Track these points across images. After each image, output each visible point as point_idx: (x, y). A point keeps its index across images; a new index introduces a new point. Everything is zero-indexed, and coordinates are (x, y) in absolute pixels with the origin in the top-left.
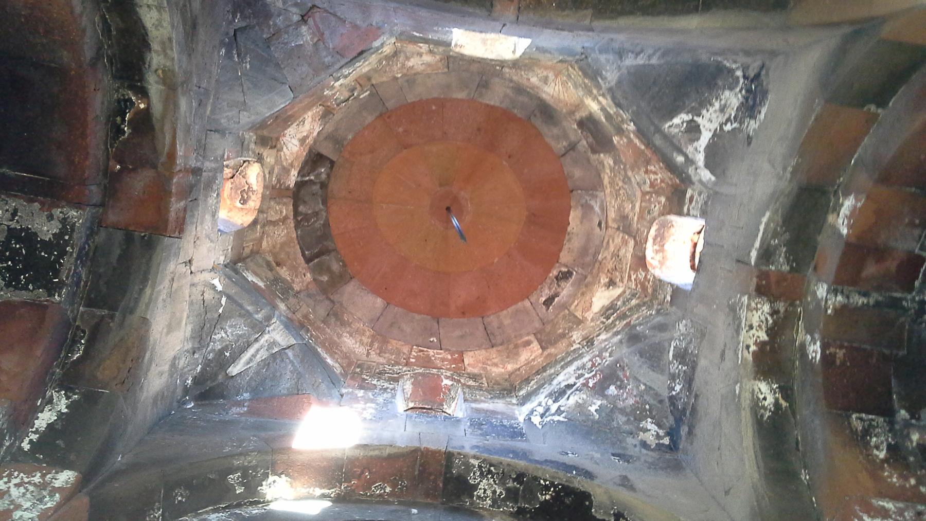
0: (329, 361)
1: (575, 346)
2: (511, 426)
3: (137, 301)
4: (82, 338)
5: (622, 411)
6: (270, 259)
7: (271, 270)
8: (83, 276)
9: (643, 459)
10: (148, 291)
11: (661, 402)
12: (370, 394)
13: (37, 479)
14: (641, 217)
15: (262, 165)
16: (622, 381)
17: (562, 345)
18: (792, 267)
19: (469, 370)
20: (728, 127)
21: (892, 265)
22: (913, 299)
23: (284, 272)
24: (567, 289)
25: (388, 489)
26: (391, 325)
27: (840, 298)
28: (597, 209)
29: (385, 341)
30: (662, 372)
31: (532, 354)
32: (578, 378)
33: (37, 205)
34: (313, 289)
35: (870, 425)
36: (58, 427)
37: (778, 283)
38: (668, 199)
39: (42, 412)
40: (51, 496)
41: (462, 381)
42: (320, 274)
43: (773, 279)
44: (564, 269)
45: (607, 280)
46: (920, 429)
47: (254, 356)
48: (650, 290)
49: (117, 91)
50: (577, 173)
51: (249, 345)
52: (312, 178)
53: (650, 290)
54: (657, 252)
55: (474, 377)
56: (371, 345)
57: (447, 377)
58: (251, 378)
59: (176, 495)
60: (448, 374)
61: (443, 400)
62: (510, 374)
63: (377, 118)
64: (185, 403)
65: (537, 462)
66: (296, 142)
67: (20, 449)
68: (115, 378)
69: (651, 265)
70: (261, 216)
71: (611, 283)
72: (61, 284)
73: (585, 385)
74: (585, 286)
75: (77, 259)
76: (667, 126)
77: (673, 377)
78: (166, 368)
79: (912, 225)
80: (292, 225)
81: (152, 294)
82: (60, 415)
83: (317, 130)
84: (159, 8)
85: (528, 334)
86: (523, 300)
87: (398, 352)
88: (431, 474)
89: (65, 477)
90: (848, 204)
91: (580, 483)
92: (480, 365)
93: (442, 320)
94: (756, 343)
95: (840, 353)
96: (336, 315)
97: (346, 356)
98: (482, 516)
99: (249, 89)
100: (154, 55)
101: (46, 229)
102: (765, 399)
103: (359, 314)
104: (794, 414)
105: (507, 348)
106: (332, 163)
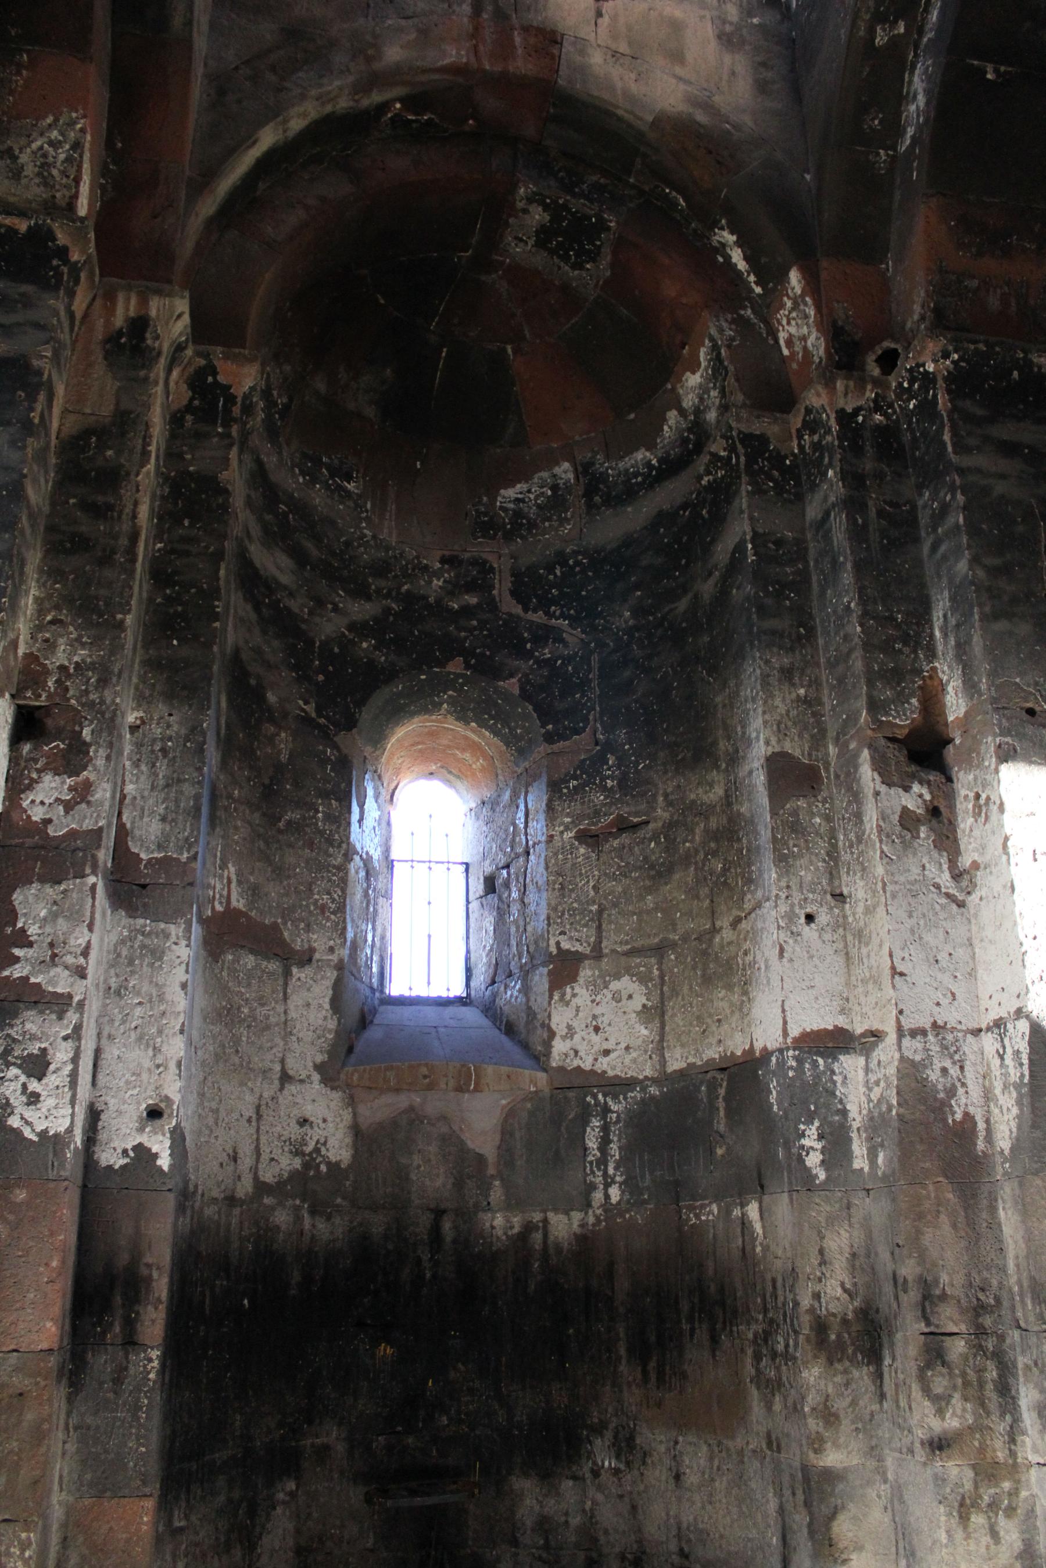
3: (630, 126)
8: (594, 178)
10: (620, 112)
13: (789, 304)
33: (511, 221)
40: (806, 304)
59: (870, 127)
67: (759, 295)
75: (574, 195)
78: (727, 59)
81: (626, 111)
82: (738, 244)
84: (286, 121)
89: (795, 279)
100: (338, 107)
101: (538, 216)
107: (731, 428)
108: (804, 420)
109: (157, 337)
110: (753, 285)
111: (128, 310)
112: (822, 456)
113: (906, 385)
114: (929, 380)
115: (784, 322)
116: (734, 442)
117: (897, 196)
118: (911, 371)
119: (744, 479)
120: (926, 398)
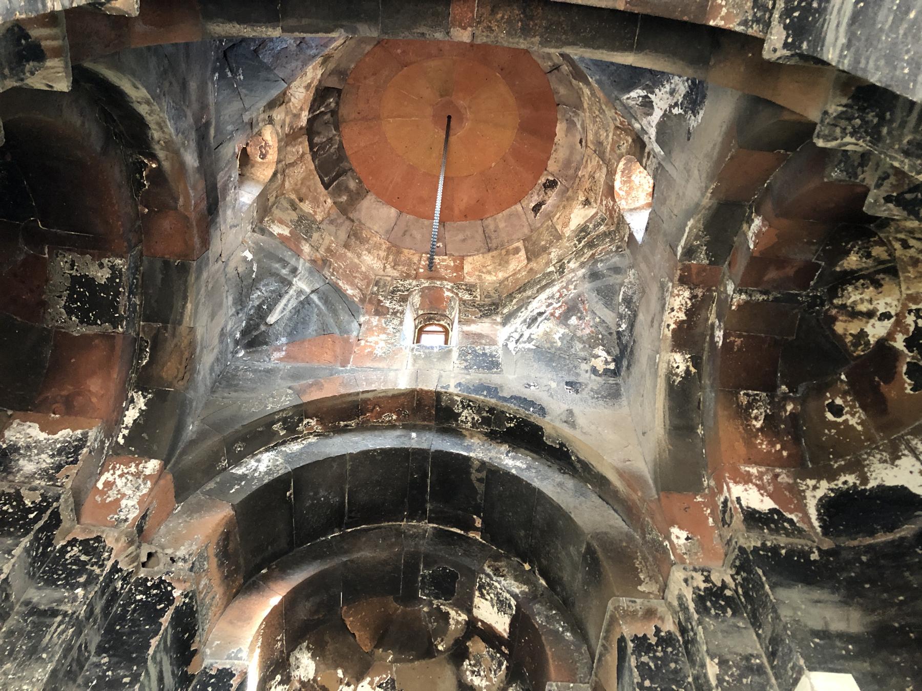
0: (350, 292)
1: (552, 269)
2: (492, 356)
3: (182, 314)
4: (146, 347)
5: (580, 339)
6: (293, 196)
7: (295, 209)
9: (589, 387)
10: (189, 306)
11: (611, 334)
12: (383, 321)
13: (133, 469)
14: (612, 150)
15: (274, 125)
16: (582, 313)
17: (542, 260)
18: (710, 260)
19: (469, 280)
20: (676, 111)
21: (790, 271)
22: (807, 296)
23: (306, 207)
24: (552, 198)
25: (395, 417)
26: (404, 234)
27: (743, 296)
28: (579, 126)
29: (399, 252)
30: (613, 310)
31: (518, 262)
32: (548, 306)
34: (335, 212)
35: (754, 399)
36: (141, 422)
37: (698, 273)
38: (633, 140)
39: (128, 410)
40: (145, 484)
41: (460, 294)
42: (340, 196)
43: (694, 271)
44: (551, 178)
45: (584, 198)
46: (793, 400)
47: (286, 305)
48: (615, 220)
49: (131, 156)
50: (562, 91)
51: (281, 296)
52: (323, 109)
53: (615, 220)
54: (624, 183)
55: (470, 289)
56: (387, 258)
57: (448, 290)
58: (286, 324)
60: (449, 287)
61: (446, 307)
62: (501, 282)
63: (375, 46)
64: (237, 352)
65: (505, 399)
66: (303, 90)
67: (117, 443)
68: (176, 377)
69: (619, 194)
70: (280, 166)
71: (587, 203)
72: (121, 319)
73: (552, 314)
74: (567, 199)
76: (625, 97)
77: (621, 317)
79: (810, 243)
80: (310, 158)
82: (141, 411)
83: (319, 72)
85: (518, 240)
86: (516, 204)
87: (409, 263)
88: (426, 406)
89: (152, 466)
90: (757, 222)
91: (535, 419)
92: (477, 273)
93: (448, 224)
94: (675, 323)
95: (738, 341)
96: (356, 236)
97: (365, 277)
98: (465, 436)
99: (246, 95)
102: (678, 367)
103: (376, 228)
104: (700, 379)
105: (500, 254)
106: (339, 91)
107: (57, 499)
108: (88, 540)
109: (32, 74)
110: (121, 435)
111: (46, 39)
112: (79, 573)
113: (149, 584)
114: (167, 598)
115: (118, 472)
116: (47, 507)
117: (211, 485)
118: (162, 581)
119: (31, 536)
120: (155, 604)
